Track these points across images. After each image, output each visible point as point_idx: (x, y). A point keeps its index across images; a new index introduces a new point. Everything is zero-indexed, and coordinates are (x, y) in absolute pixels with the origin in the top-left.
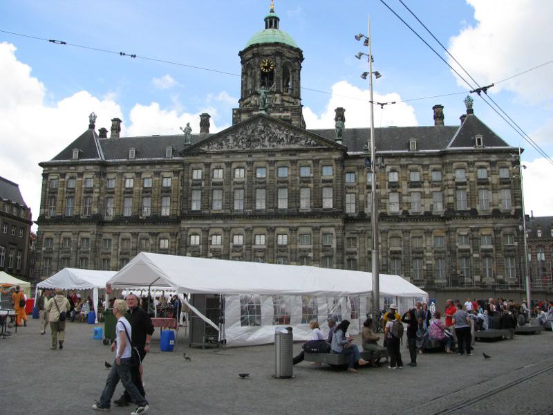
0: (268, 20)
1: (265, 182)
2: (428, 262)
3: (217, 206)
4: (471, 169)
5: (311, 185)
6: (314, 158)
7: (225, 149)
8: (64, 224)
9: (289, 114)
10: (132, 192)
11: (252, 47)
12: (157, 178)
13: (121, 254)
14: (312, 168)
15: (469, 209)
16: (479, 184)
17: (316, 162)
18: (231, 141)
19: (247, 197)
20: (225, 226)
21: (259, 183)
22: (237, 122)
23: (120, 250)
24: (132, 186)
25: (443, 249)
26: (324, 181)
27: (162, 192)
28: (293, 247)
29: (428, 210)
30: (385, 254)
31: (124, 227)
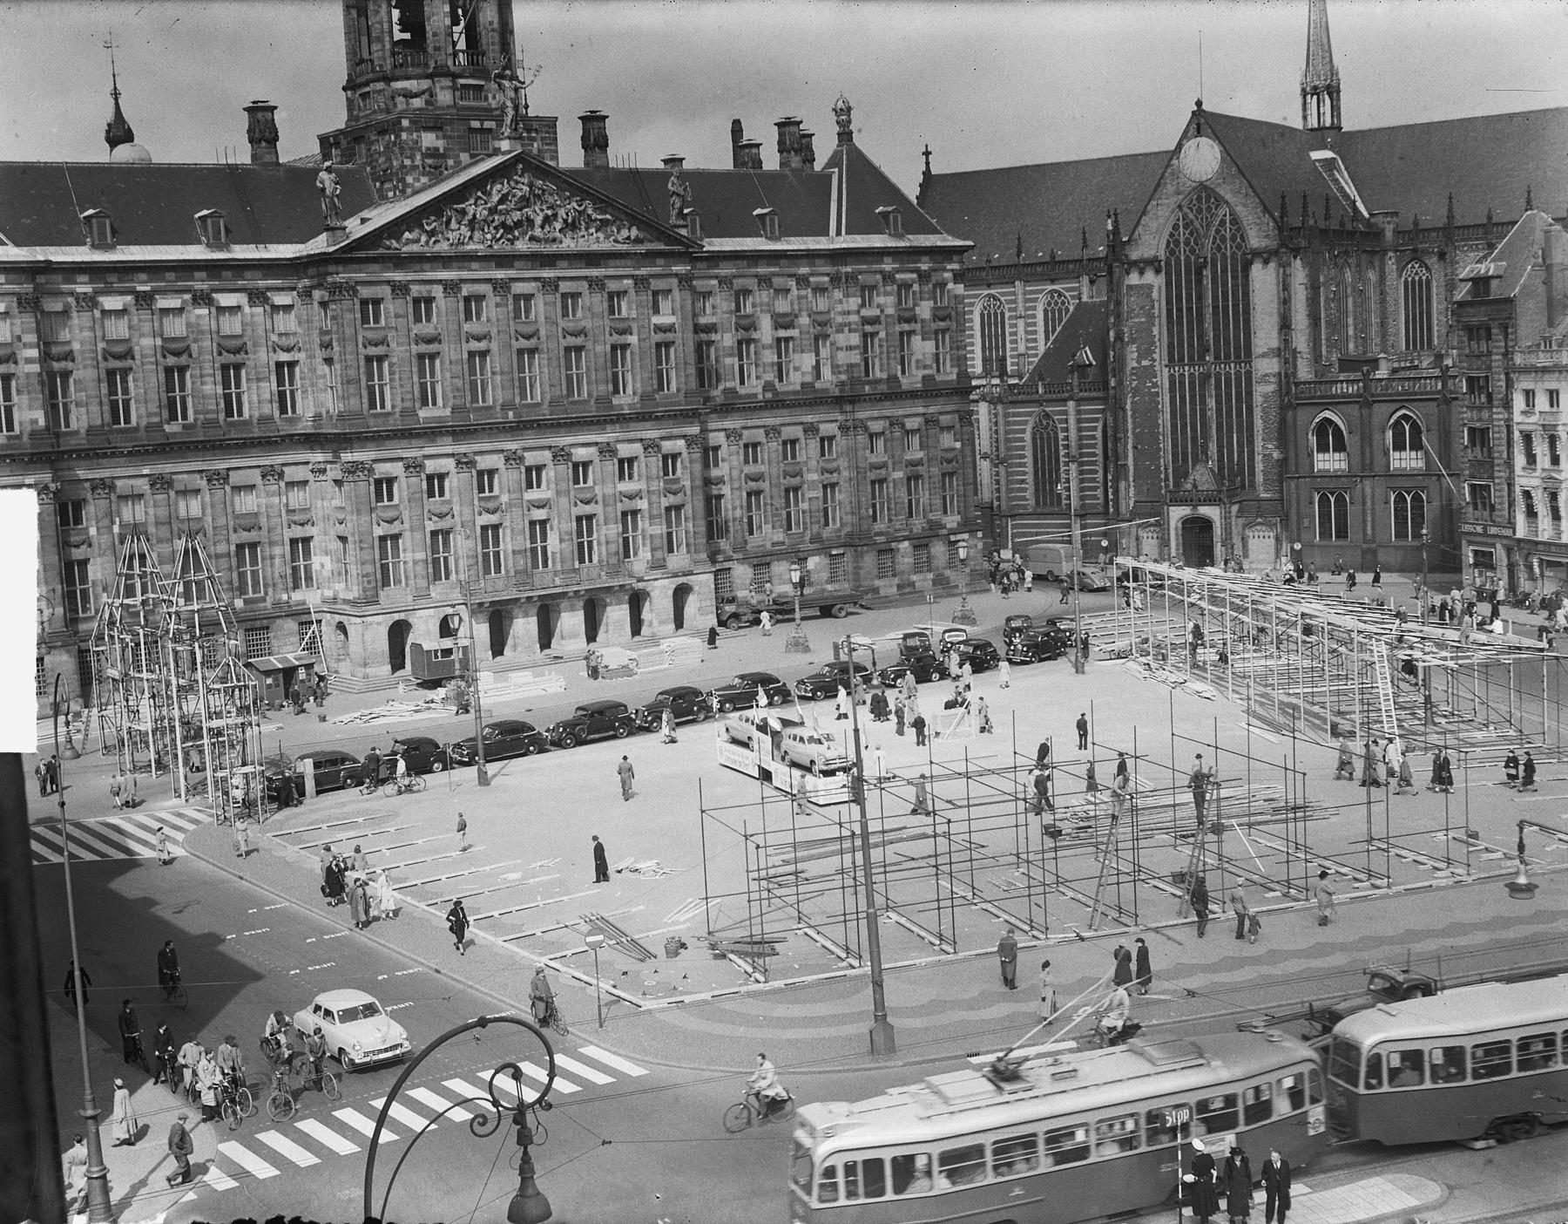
1: (535, 334)
2: (813, 494)
5: (633, 339)
12: (204, 311)
15: (884, 376)
16: (902, 320)
17: (641, 282)
18: (454, 225)
19: (502, 373)
20: (462, 449)
21: (528, 337)
22: (412, 158)
23: (116, 529)
25: (834, 465)
26: (659, 329)
27: (220, 354)
28: (609, 490)
29: (808, 379)
30: (736, 485)
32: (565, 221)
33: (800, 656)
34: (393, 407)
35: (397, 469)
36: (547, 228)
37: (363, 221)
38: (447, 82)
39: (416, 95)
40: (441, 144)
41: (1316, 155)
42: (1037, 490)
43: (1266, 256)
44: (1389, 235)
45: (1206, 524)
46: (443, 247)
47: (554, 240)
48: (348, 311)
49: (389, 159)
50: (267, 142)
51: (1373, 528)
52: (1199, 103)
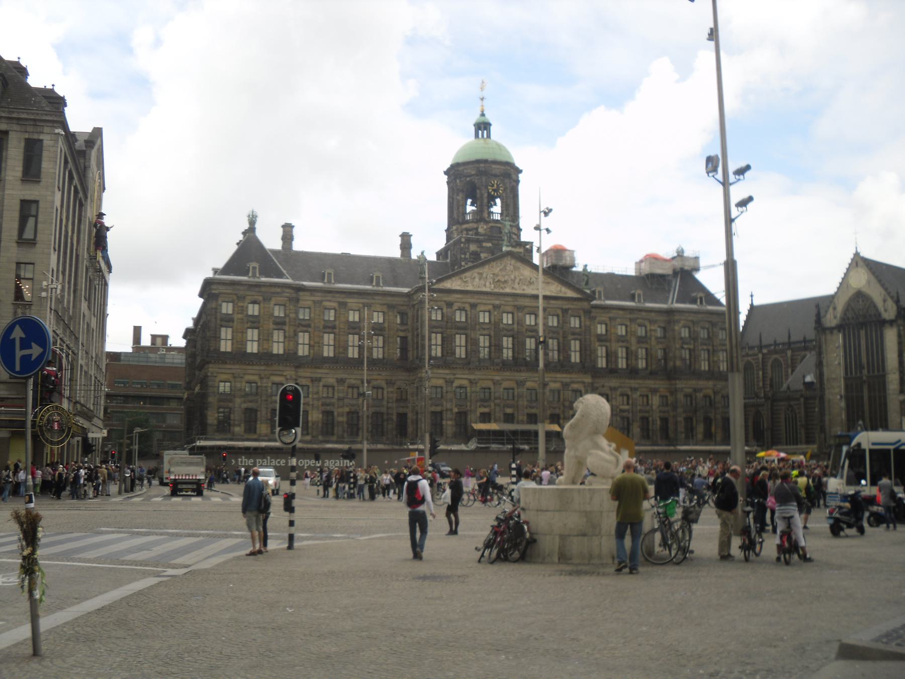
1: (513, 330)
3: (460, 352)
4: (696, 329)
6: (564, 307)
7: (470, 288)
8: (249, 364)
9: (521, 250)
10: (334, 327)
11: (478, 162)
13: (323, 405)
14: (561, 318)
18: (477, 280)
20: (472, 377)
22: (465, 254)
24: (332, 319)
25: (666, 409)
26: (573, 334)
31: (327, 371)
34: (443, 355)
35: (440, 382)
39: (470, 230)
40: (478, 250)
43: (891, 323)
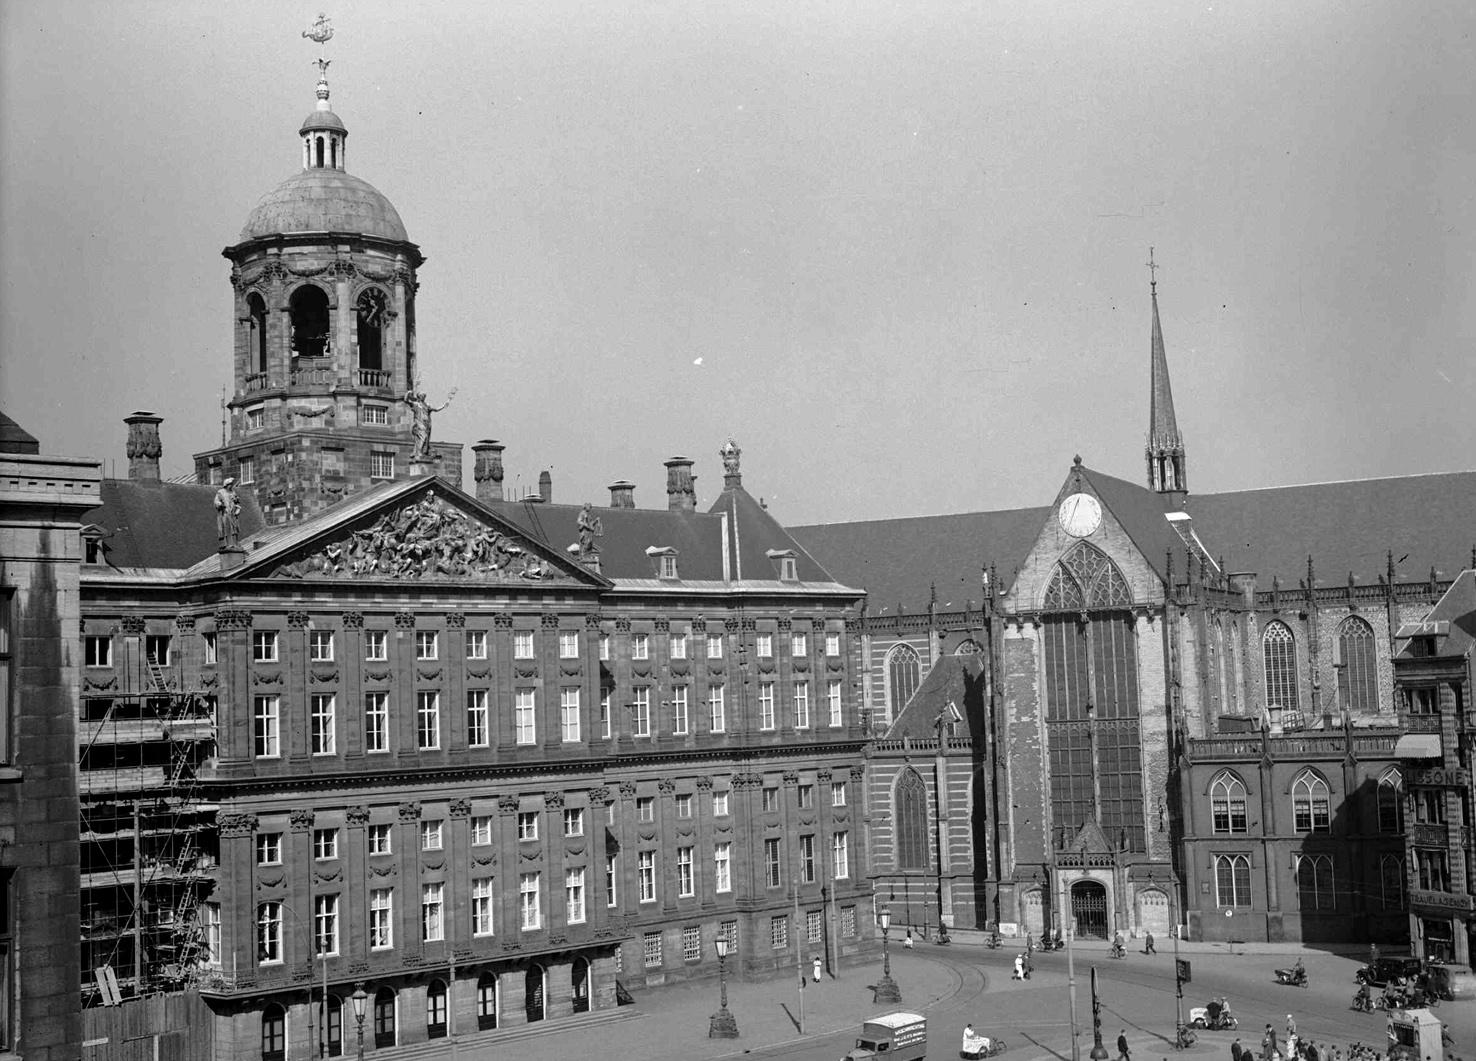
0: (325, 136)
5: (539, 682)
18: (359, 552)
22: (310, 479)
32: (475, 553)
33: (727, 1042)
36: (456, 557)
37: (257, 545)
38: (352, 401)
39: (315, 415)
40: (341, 467)
41: (1171, 517)
42: (901, 851)
44: (1249, 596)
45: (1098, 890)
46: (346, 577)
47: (463, 572)
48: (237, 639)
49: (283, 481)
50: (149, 456)
51: (1278, 896)
52: (1077, 461)
